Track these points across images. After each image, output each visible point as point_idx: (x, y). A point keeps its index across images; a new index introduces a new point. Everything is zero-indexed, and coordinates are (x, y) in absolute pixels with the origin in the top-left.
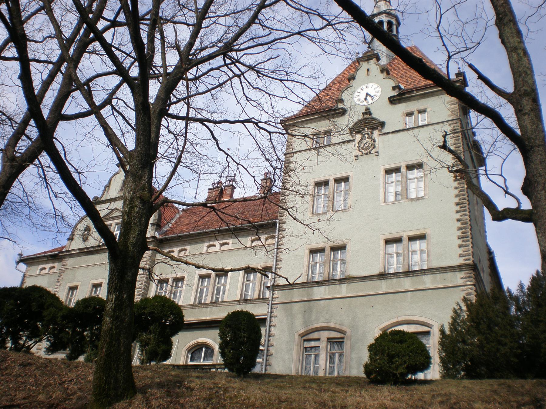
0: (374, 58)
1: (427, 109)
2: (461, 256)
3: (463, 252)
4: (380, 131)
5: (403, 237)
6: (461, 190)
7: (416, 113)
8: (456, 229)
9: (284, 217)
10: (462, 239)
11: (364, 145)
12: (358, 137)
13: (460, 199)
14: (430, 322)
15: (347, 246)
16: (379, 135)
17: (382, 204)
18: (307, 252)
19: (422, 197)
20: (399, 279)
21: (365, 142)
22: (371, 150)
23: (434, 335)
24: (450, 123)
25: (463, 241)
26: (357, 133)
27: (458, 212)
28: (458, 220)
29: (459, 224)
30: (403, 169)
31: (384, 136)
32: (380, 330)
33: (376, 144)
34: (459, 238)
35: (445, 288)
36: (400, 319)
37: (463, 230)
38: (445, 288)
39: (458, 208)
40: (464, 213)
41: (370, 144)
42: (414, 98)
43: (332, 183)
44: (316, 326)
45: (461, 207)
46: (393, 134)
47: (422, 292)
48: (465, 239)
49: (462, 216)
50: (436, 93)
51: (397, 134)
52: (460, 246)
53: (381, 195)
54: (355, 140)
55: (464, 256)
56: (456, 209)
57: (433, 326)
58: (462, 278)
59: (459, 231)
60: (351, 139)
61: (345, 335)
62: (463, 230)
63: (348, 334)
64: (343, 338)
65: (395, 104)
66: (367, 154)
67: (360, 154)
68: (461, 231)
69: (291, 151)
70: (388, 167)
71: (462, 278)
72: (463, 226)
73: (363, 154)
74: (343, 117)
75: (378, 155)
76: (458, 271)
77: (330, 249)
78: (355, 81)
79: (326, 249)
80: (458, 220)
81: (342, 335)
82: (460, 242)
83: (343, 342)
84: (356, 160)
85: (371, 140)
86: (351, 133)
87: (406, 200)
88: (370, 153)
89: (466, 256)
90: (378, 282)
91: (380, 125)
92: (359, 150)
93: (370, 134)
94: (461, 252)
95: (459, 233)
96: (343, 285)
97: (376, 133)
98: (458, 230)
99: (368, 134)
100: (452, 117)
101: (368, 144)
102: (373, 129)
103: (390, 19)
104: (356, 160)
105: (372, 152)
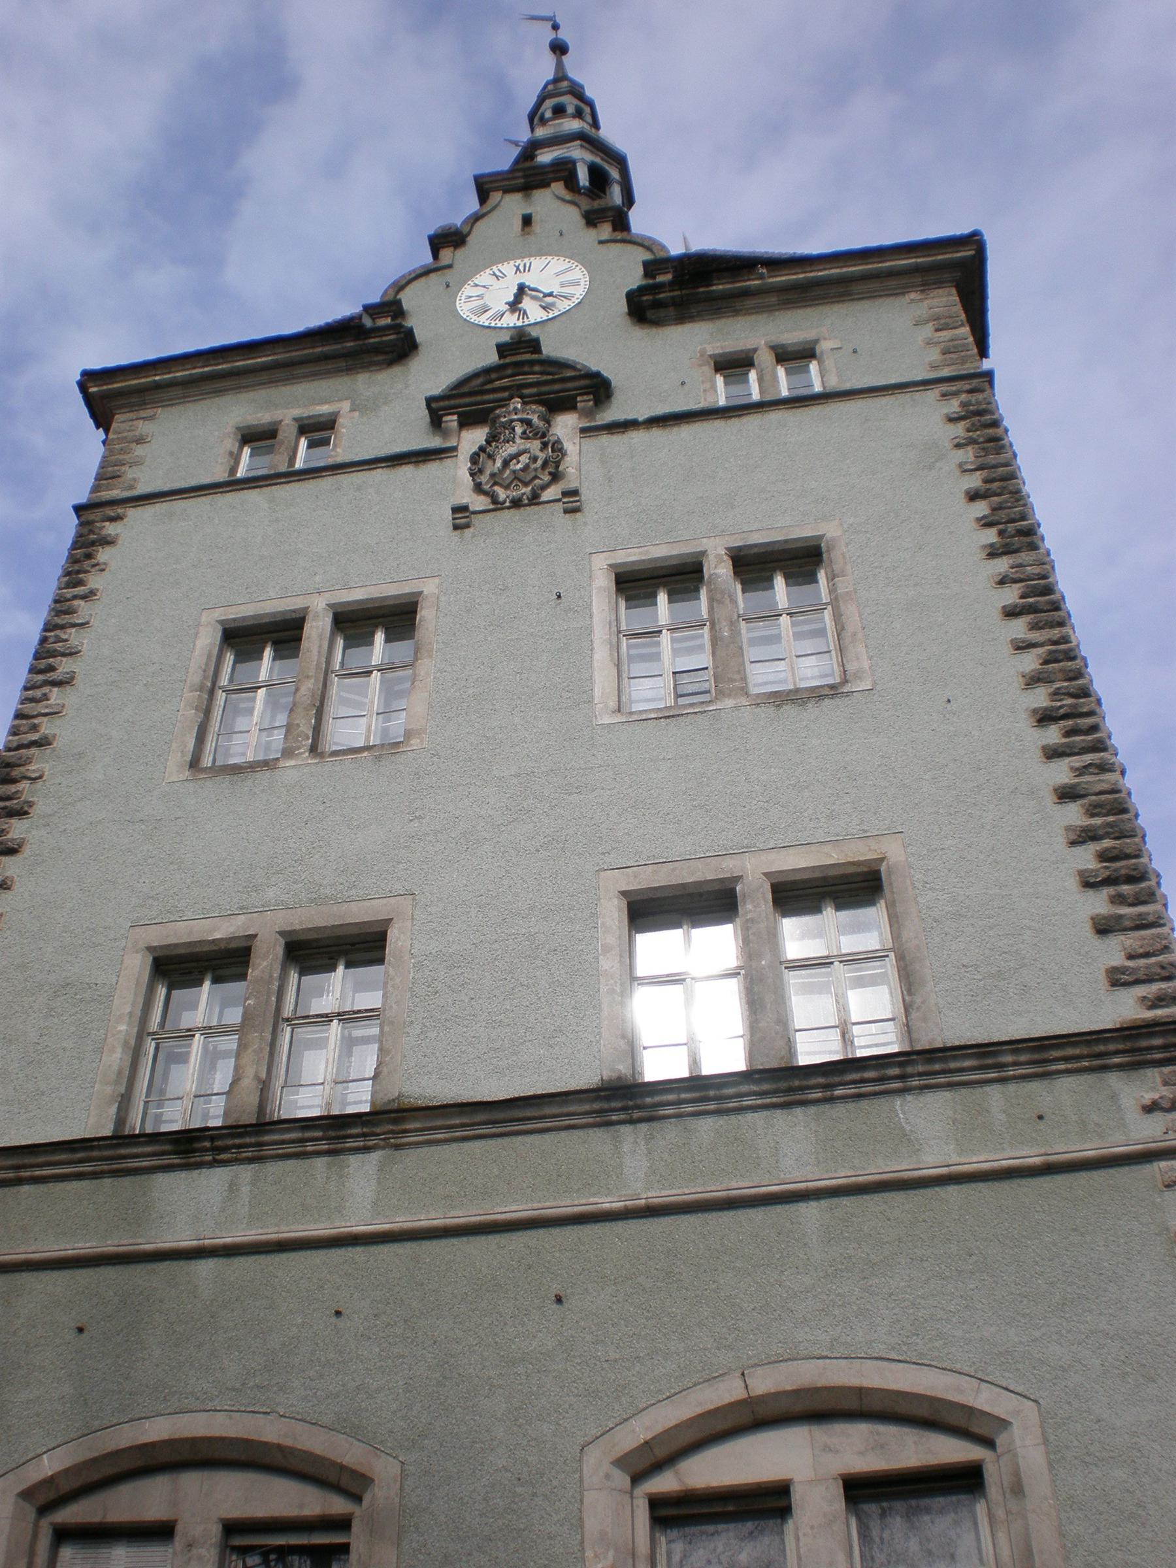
0: (556, 180)
1: (817, 341)
2: (1118, 979)
3: (1131, 957)
4: (588, 414)
5: (738, 879)
6: (1050, 652)
7: (765, 358)
8: (1060, 841)
9: (24, 785)
10: (1106, 892)
11: (506, 463)
12: (474, 438)
13: (1056, 694)
14: (984, 1399)
15: (396, 939)
16: (583, 430)
17: (607, 720)
18: (138, 966)
19: (832, 687)
20: (734, 1119)
21: (511, 449)
22: (544, 488)
23: (1017, 1489)
24: (944, 388)
25: (1118, 900)
26: (468, 421)
27: (1052, 754)
28: (1066, 794)
29: (1074, 814)
30: (719, 570)
31: (605, 439)
32: (620, 1463)
33: (570, 464)
34: (1089, 883)
35: (1049, 1169)
36: (764, 1383)
37: (1107, 843)
38: (1049, 1169)
39: (1053, 735)
40: (1088, 758)
41: (534, 459)
42: (750, 302)
43: (318, 628)
44: (157, 1430)
45: (1068, 733)
46: (656, 433)
47: (899, 1197)
48: (1125, 889)
49: (1081, 771)
50: (858, 288)
51: (675, 430)
52: (1103, 928)
53: (598, 677)
54: (455, 449)
55: (1138, 982)
56: (1044, 742)
57: (1004, 1424)
58: (1151, 1108)
59: (1079, 850)
60: (435, 442)
61: (357, 1498)
62: (1107, 843)
63: (381, 1494)
64: (343, 1524)
65: (657, 323)
66: (516, 504)
67: (479, 503)
68: (1093, 848)
69: (116, 493)
70: (632, 556)
71: (1151, 1108)
72: (1098, 821)
73: (495, 500)
74: (397, 370)
75: (576, 510)
76: (1120, 1067)
77: (280, 950)
78: (461, 253)
79: (259, 948)
80: (1066, 794)
81: (338, 1505)
82: (1099, 903)
83: (345, 1549)
84: (456, 527)
85: (545, 445)
86: (436, 422)
87: (744, 701)
88: (534, 499)
89: (1149, 980)
90: (597, 1141)
91: (585, 390)
92: (478, 488)
93: (535, 419)
94: (1119, 960)
95: (1086, 858)
96: (354, 1160)
97: (565, 426)
98: (1073, 843)
99: (528, 423)
100: (953, 367)
101: (524, 459)
102: (557, 405)
103: (598, 160)
104: (456, 527)
105: (549, 494)
